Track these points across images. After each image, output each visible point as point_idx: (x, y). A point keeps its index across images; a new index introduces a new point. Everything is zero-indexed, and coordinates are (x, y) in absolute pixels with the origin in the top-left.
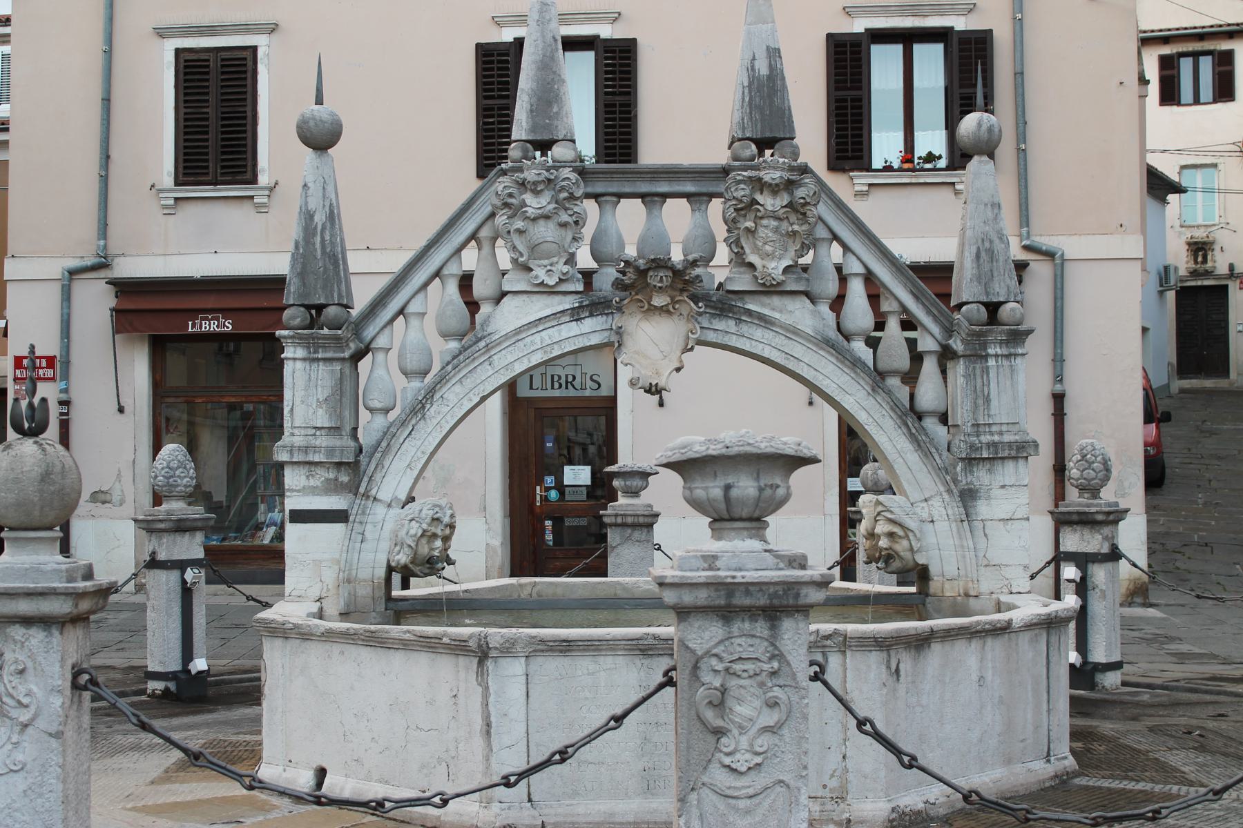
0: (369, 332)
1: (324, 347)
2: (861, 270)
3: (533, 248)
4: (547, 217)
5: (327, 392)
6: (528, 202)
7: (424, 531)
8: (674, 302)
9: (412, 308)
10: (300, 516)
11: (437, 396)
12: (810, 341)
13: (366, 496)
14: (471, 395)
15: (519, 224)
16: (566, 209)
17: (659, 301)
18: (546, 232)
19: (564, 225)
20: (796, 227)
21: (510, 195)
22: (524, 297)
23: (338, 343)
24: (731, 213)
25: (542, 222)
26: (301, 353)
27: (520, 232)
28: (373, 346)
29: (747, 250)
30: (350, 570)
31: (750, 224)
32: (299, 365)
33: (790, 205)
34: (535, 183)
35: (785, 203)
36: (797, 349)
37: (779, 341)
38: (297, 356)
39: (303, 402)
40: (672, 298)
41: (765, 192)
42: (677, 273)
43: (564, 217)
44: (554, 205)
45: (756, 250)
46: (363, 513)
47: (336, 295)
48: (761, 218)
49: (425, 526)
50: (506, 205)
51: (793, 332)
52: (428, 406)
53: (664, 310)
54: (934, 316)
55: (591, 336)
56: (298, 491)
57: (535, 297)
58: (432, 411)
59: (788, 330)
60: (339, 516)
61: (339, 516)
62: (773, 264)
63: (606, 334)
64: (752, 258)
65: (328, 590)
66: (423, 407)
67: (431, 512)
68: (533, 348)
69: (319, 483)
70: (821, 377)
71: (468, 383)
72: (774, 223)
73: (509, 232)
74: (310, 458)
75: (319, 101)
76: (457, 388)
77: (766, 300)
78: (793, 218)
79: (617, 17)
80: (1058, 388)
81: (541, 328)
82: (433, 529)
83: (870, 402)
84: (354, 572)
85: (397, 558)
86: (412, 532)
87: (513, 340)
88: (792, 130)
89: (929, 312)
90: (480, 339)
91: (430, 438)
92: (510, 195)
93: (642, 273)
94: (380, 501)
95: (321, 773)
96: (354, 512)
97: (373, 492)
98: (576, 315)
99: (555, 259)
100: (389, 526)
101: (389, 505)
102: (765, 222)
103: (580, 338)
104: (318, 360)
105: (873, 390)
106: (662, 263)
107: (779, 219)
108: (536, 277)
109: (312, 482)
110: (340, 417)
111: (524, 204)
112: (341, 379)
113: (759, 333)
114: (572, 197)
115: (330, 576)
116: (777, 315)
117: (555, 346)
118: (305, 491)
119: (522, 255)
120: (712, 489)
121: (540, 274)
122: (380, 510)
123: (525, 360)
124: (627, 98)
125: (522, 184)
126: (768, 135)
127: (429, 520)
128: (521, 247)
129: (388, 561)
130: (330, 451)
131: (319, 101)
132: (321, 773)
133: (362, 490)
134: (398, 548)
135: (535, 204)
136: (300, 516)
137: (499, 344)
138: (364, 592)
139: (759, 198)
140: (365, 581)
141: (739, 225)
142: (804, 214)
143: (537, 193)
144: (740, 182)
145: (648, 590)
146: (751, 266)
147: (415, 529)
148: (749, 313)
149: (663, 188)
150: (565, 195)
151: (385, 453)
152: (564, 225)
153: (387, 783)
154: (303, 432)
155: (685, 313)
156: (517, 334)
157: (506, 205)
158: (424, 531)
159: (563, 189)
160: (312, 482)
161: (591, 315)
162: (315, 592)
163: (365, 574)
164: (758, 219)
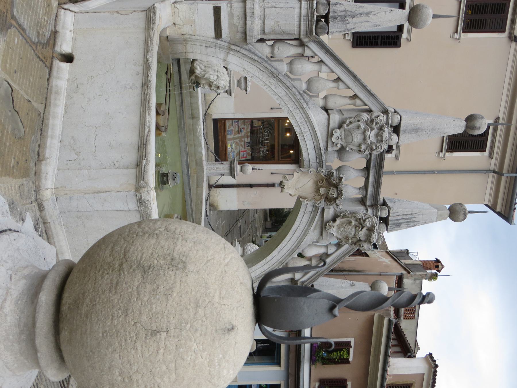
0: (313, 46)
1: (307, 25)
2: (329, 253)
3: (350, 131)
4: (365, 139)
5: (283, 27)
6: (373, 132)
7: (212, 83)
8: (322, 196)
9: (324, 68)
10: (217, 11)
11: (280, 84)
12: (301, 239)
13: (230, 49)
14: (280, 99)
15: (362, 126)
16: (367, 147)
17: (322, 191)
18: (357, 138)
19: (359, 146)
20: (350, 241)
21: (377, 123)
22: (326, 124)
23: (309, 33)
24: (359, 216)
25: (362, 137)
26: (304, 12)
27: (359, 127)
28: (306, 48)
29: (342, 220)
30: (191, 41)
31: (354, 223)
32: (297, 11)
33: (360, 240)
34: (382, 137)
35: (361, 239)
36: (297, 234)
37: (302, 227)
38: (302, 9)
39: (278, 13)
40: (323, 195)
41: (367, 231)
42: (335, 200)
43: (363, 147)
44: (369, 142)
45: (341, 224)
46: (220, 47)
47: (333, 30)
48: (356, 228)
49: (215, 83)
50: (372, 121)
51: (305, 233)
52: (275, 79)
53: (317, 190)
54: (309, 279)
55: (307, 153)
56: (231, 10)
57: (326, 129)
58: (273, 81)
59: (306, 231)
60: (218, 34)
61: (218, 34)
62: (335, 229)
63: (307, 159)
64: (338, 221)
65: (179, 28)
66: (274, 77)
67: (222, 85)
68: (302, 128)
69: (235, 22)
70: (286, 243)
71: (286, 99)
72: (353, 233)
73: (359, 121)
74: (248, 19)
75: (435, 16)
76: (283, 93)
77: (319, 223)
78: (355, 240)
79: (408, 40)
80: (276, 185)
81: (311, 132)
82: (213, 86)
83: (275, 260)
84: (190, 43)
85: (198, 67)
86: (212, 77)
87: (306, 119)
88: (392, 230)
89: (311, 277)
90: (307, 104)
91: (259, 80)
92: (377, 123)
93: (336, 186)
94: (227, 55)
95: (69, 58)
96: (221, 43)
97: (231, 52)
98: (317, 148)
99: (344, 140)
100: (215, 61)
101: (225, 60)
102: (354, 229)
103: (306, 149)
104: (300, 21)
105: (281, 262)
106: (340, 196)
107: (355, 235)
108: (336, 132)
109: (235, 18)
110: (269, 34)
111: (372, 129)
112: (290, 34)
113: (305, 220)
114: (372, 150)
115: (187, 29)
116: (313, 228)
117: (302, 138)
118: (231, 15)
119: (348, 125)
120: (243, 81)
121: (337, 133)
122: (222, 55)
123: (296, 124)
124: (380, 44)
125: (381, 129)
126: (390, 222)
127: (218, 85)
128: (351, 126)
129: (196, 60)
130: (252, 30)
131: (435, 16)
132: (69, 58)
133: (233, 47)
134: (203, 68)
135: (372, 135)
136: (217, 11)
137: (304, 113)
138: (180, 48)
139: (364, 229)
140: (186, 48)
141: (353, 218)
142: (355, 244)
143: (377, 135)
144: (373, 221)
145: (197, 130)
146: (334, 220)
147: (213, 78)
148: (314, 217)
149: (371, 179)
150: (374, 148)
151: (252, 59)
152: (359, 146)
153: (65, 112)
154: (262, 13)
155: (315, 197)
156: (309, 122)
157: (372, 121)
158: (212, 83)
159: (377, 147)
160: (235, 18)
161: (316, 154)
162: (178, 21)
163: (189, 48)
164: (356, 227)
